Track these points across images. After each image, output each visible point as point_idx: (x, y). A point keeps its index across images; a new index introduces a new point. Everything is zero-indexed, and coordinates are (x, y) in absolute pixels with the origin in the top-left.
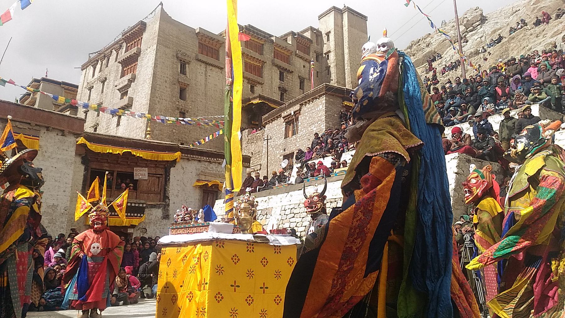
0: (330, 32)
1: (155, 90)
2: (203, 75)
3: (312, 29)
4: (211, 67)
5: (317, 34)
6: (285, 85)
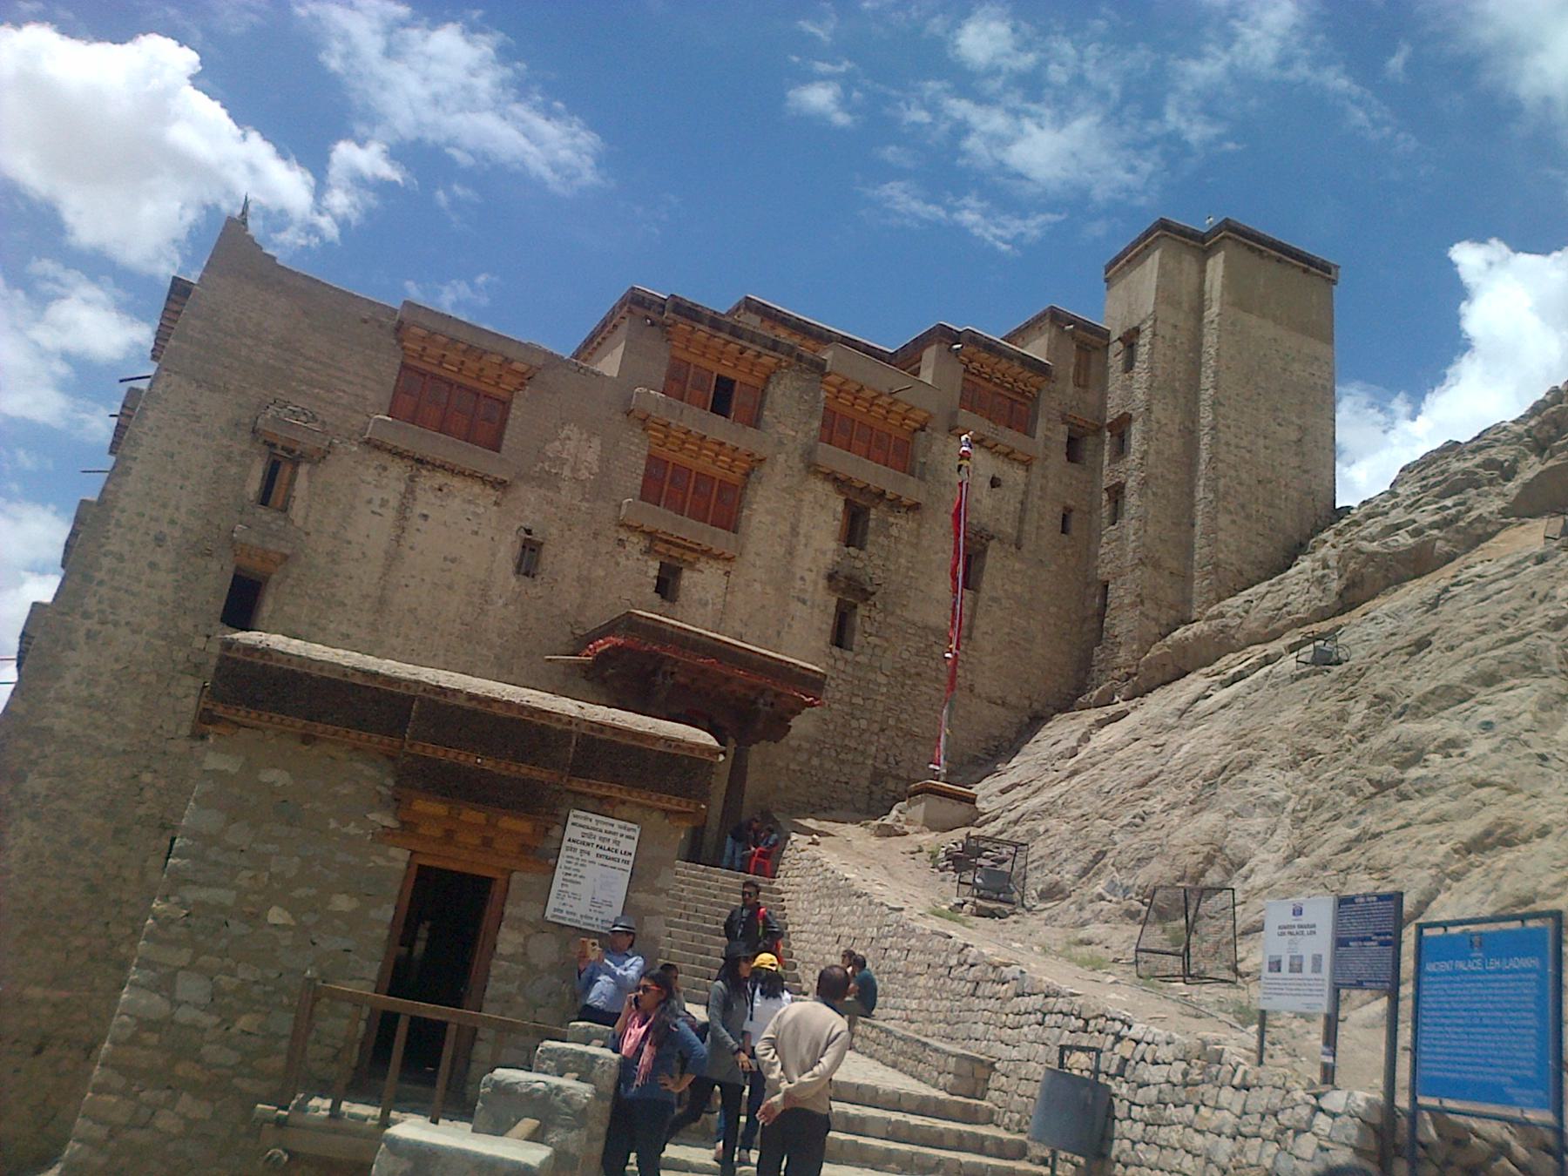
0: (1136, 331)
1: (87, 578)
2: (390, 514)
3: (1055, 317)
4: (440, 478)
5: (1087, 342)
6: (869, 563)
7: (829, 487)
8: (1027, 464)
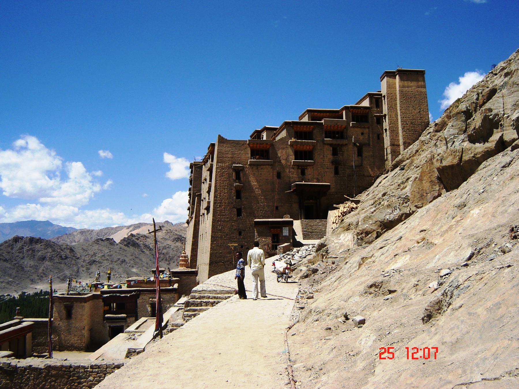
4: (262, 167)
7: (329, 146)
8: (368, 128)
